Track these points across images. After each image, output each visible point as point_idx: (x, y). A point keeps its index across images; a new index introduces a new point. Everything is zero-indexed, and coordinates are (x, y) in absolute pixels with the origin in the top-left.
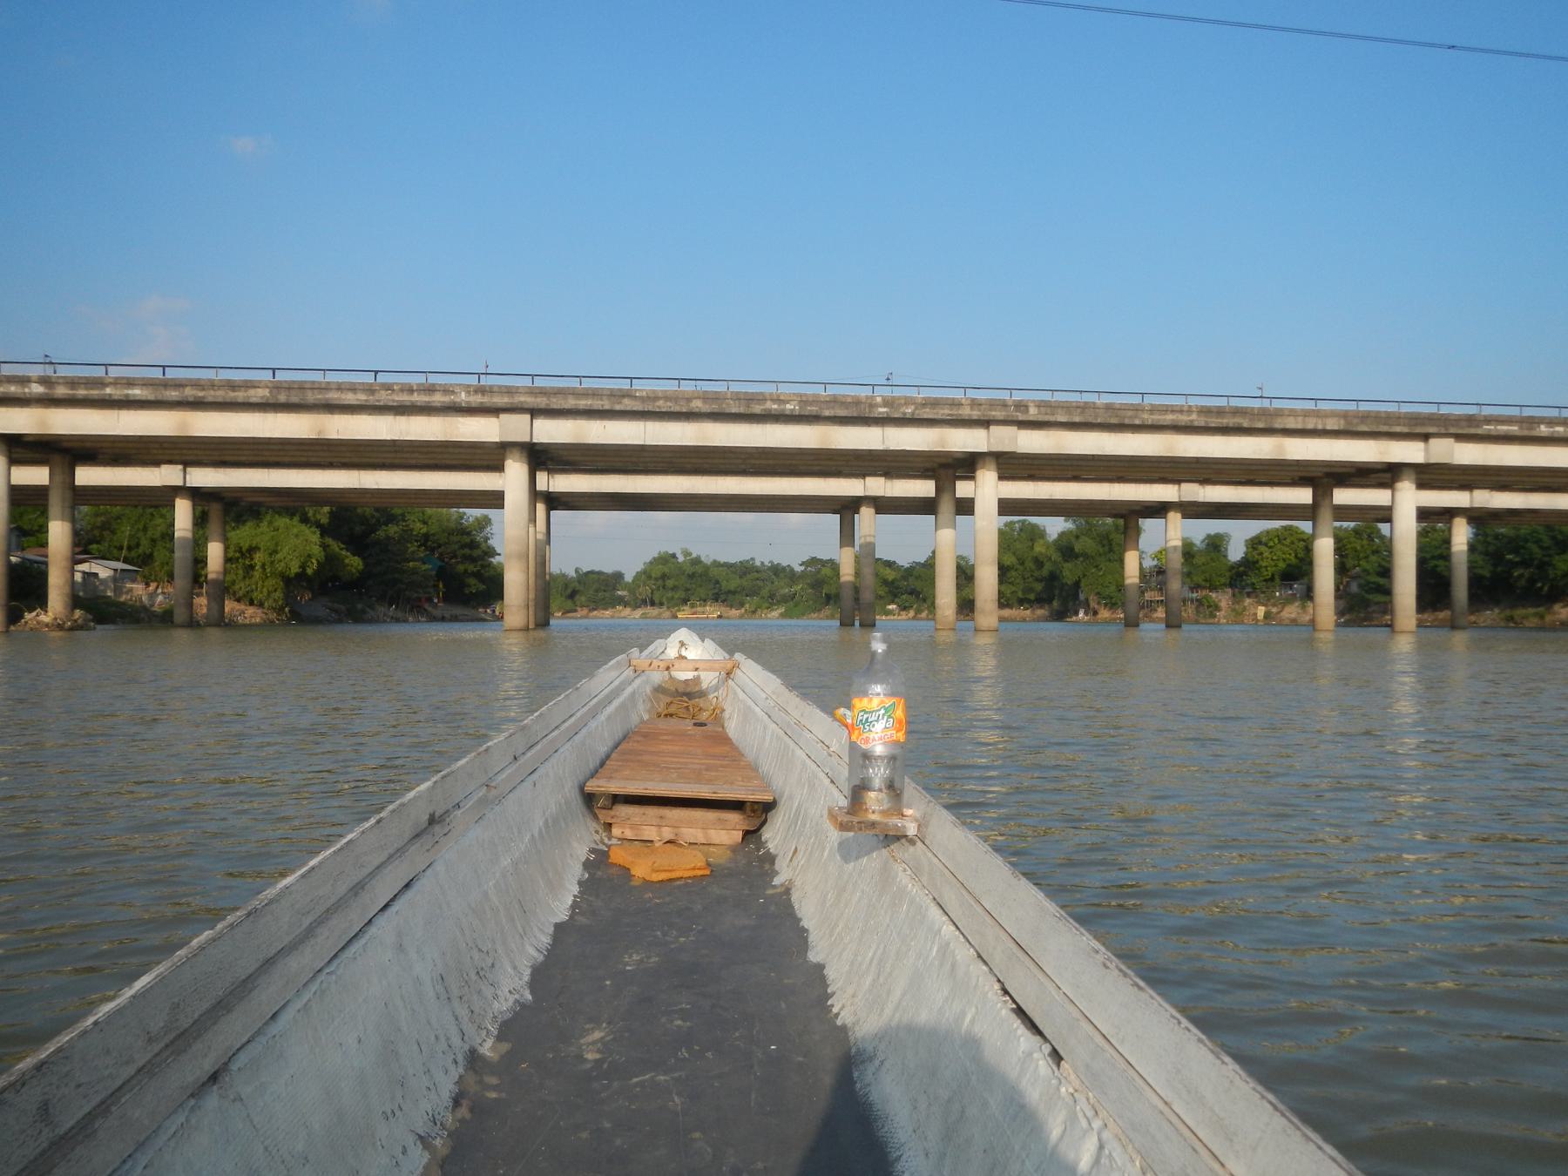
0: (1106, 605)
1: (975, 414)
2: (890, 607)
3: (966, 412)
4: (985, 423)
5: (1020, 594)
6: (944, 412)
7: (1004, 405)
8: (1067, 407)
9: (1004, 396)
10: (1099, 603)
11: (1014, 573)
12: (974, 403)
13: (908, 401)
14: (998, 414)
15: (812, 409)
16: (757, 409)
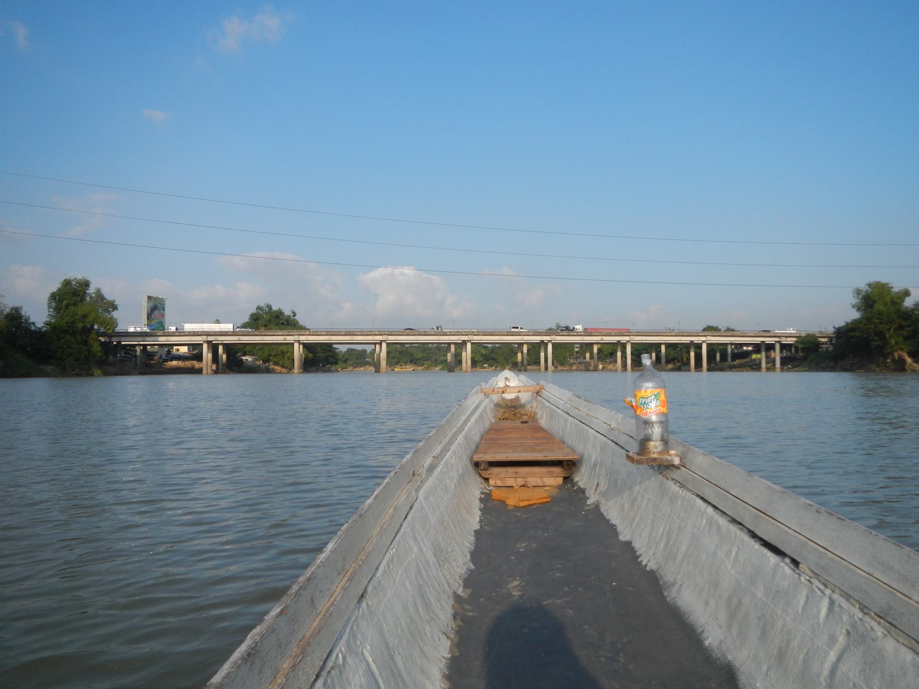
0: (560, 365)
1: (465, 334)
2: (485, 365)
3: (463, 333)
4: (467, 335)
5: (534, 360)
6: (460, 333)
7: (470, 332)
8: (482, 332)
9: (470, 330)
10: (558, 364)
11: (531, 352)
12: (465, 332)
13: (453, 332)
14: (469, 334)
15: (436, 334)
16: (427, 334)
